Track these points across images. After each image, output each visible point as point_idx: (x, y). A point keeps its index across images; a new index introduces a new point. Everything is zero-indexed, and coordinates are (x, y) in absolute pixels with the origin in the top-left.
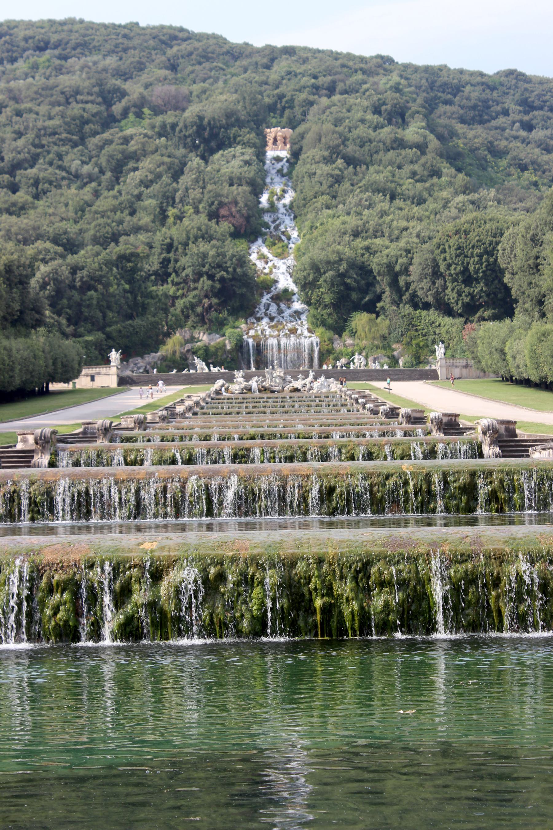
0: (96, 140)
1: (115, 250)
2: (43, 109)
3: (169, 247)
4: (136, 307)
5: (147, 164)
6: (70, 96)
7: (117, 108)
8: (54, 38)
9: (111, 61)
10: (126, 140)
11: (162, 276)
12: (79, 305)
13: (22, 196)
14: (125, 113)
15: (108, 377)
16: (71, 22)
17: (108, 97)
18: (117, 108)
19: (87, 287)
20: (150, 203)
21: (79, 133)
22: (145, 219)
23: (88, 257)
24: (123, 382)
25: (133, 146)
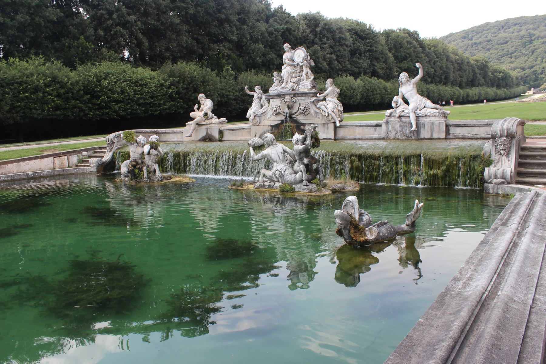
0: (528, 46)
1: (532, 70)
2: (517, 41)
3: (543, 68)
4: (536, 80)
5: (539, 50)
6: (523, 37)
7: (533, 38)
8: (518, 22)
9: (531, 26)
10: (535, 46)
11: (542, 73)
12: (525, 80)
13: (513, 59)
14: (535, 39)
15: (531, 92)
16: (521, 18)
17: (531, 36)
18: (533, 38)
19: (527, 77)
20: (539, 59)
21: (525, 45)
22: (538, 62)
23: (527, 72)
24: (534, 93)
25: (536, 47)
